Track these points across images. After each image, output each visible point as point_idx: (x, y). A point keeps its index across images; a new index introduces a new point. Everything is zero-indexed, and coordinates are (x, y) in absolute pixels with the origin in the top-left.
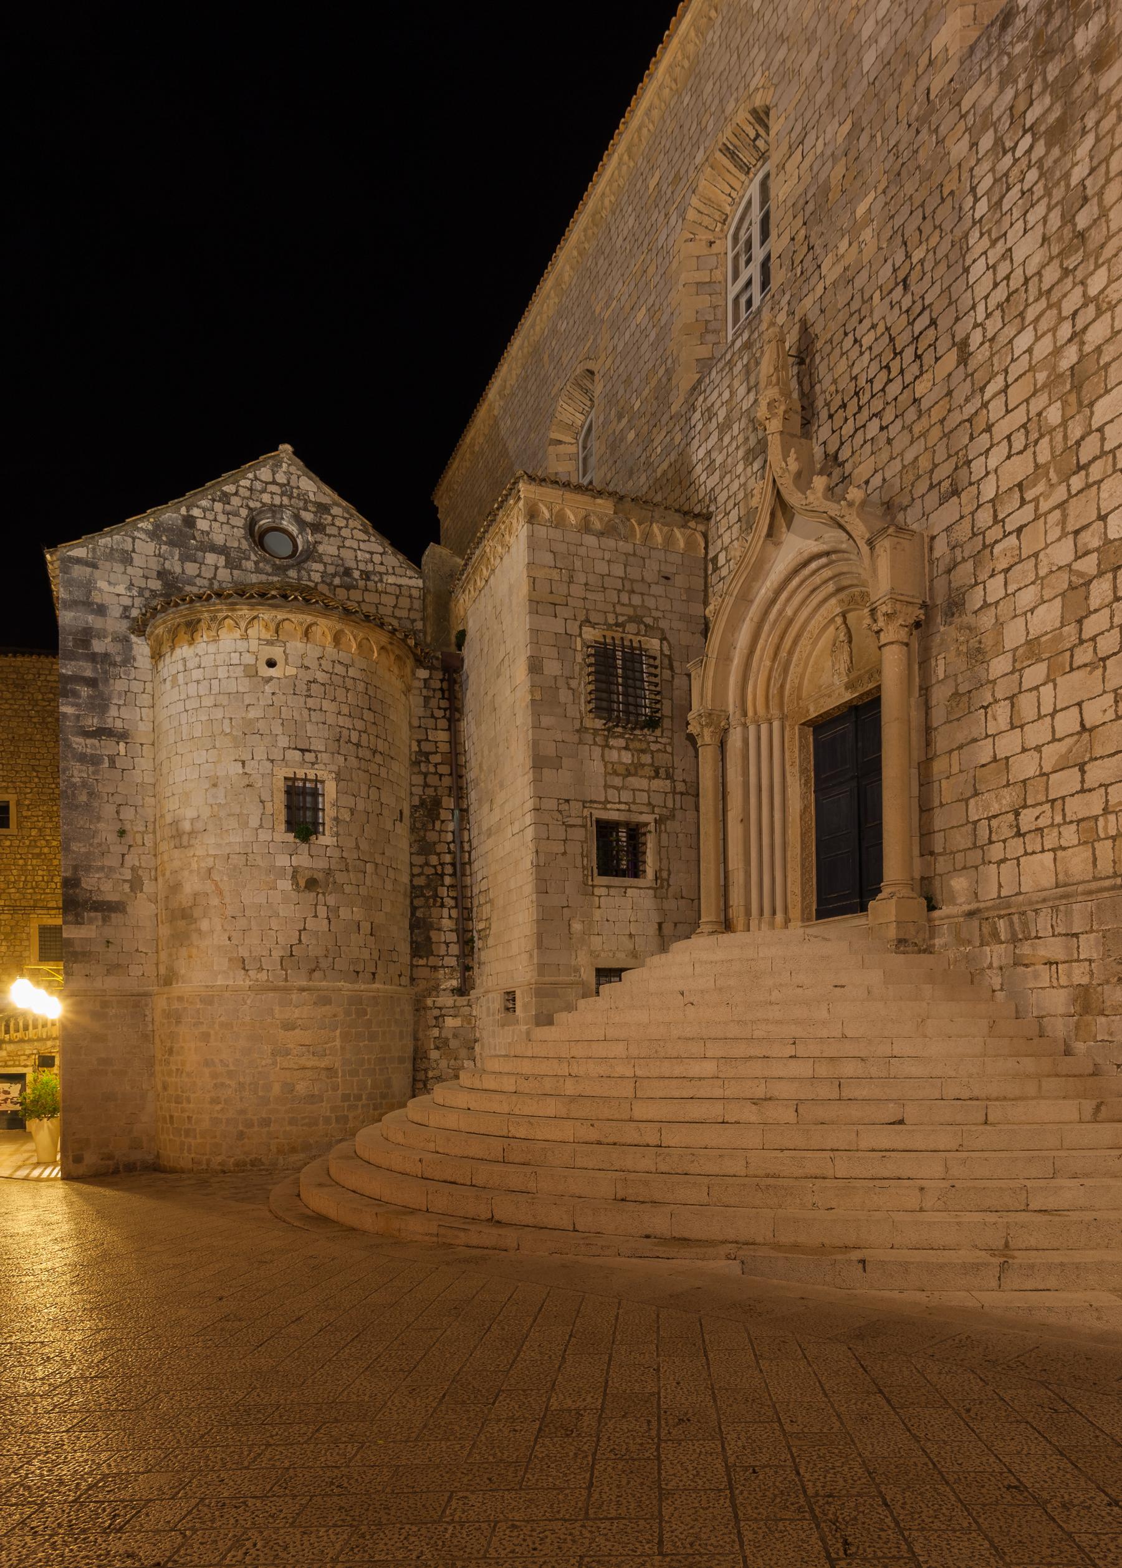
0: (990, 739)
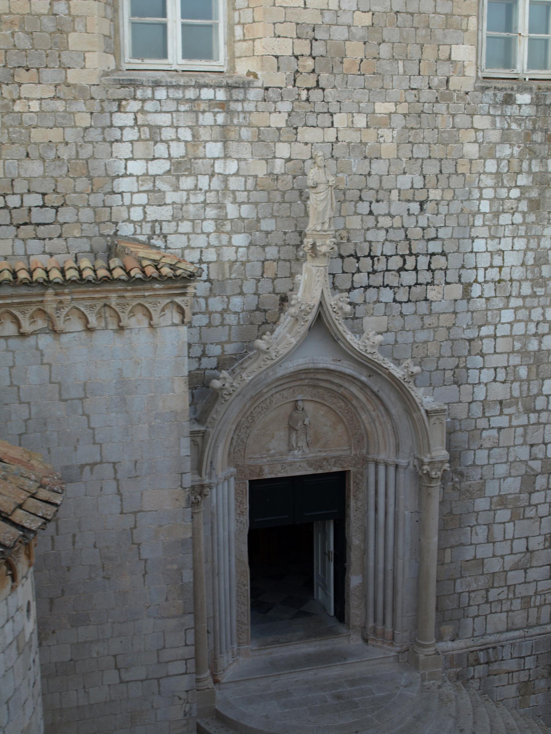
0: (474, 547)
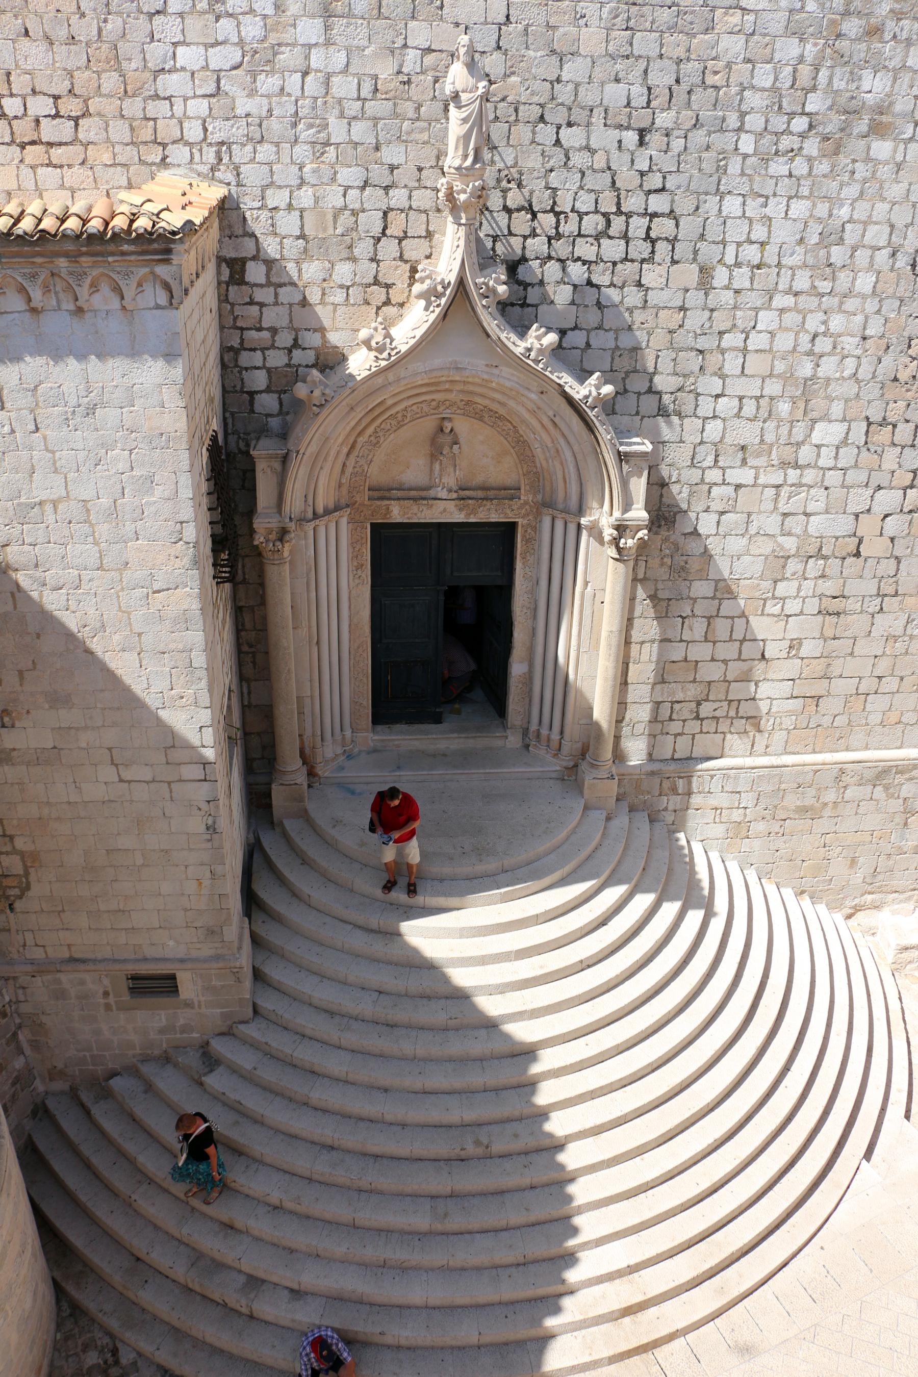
0: (685, 644)
